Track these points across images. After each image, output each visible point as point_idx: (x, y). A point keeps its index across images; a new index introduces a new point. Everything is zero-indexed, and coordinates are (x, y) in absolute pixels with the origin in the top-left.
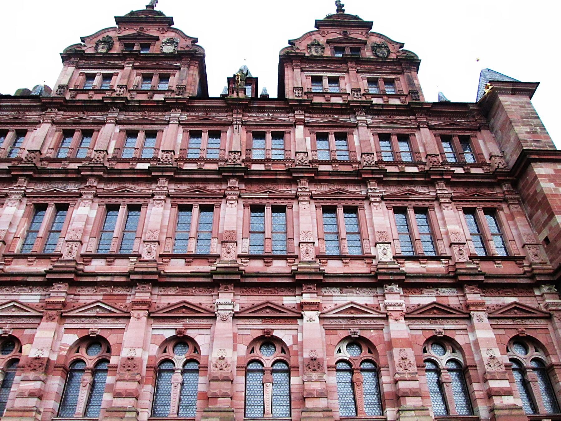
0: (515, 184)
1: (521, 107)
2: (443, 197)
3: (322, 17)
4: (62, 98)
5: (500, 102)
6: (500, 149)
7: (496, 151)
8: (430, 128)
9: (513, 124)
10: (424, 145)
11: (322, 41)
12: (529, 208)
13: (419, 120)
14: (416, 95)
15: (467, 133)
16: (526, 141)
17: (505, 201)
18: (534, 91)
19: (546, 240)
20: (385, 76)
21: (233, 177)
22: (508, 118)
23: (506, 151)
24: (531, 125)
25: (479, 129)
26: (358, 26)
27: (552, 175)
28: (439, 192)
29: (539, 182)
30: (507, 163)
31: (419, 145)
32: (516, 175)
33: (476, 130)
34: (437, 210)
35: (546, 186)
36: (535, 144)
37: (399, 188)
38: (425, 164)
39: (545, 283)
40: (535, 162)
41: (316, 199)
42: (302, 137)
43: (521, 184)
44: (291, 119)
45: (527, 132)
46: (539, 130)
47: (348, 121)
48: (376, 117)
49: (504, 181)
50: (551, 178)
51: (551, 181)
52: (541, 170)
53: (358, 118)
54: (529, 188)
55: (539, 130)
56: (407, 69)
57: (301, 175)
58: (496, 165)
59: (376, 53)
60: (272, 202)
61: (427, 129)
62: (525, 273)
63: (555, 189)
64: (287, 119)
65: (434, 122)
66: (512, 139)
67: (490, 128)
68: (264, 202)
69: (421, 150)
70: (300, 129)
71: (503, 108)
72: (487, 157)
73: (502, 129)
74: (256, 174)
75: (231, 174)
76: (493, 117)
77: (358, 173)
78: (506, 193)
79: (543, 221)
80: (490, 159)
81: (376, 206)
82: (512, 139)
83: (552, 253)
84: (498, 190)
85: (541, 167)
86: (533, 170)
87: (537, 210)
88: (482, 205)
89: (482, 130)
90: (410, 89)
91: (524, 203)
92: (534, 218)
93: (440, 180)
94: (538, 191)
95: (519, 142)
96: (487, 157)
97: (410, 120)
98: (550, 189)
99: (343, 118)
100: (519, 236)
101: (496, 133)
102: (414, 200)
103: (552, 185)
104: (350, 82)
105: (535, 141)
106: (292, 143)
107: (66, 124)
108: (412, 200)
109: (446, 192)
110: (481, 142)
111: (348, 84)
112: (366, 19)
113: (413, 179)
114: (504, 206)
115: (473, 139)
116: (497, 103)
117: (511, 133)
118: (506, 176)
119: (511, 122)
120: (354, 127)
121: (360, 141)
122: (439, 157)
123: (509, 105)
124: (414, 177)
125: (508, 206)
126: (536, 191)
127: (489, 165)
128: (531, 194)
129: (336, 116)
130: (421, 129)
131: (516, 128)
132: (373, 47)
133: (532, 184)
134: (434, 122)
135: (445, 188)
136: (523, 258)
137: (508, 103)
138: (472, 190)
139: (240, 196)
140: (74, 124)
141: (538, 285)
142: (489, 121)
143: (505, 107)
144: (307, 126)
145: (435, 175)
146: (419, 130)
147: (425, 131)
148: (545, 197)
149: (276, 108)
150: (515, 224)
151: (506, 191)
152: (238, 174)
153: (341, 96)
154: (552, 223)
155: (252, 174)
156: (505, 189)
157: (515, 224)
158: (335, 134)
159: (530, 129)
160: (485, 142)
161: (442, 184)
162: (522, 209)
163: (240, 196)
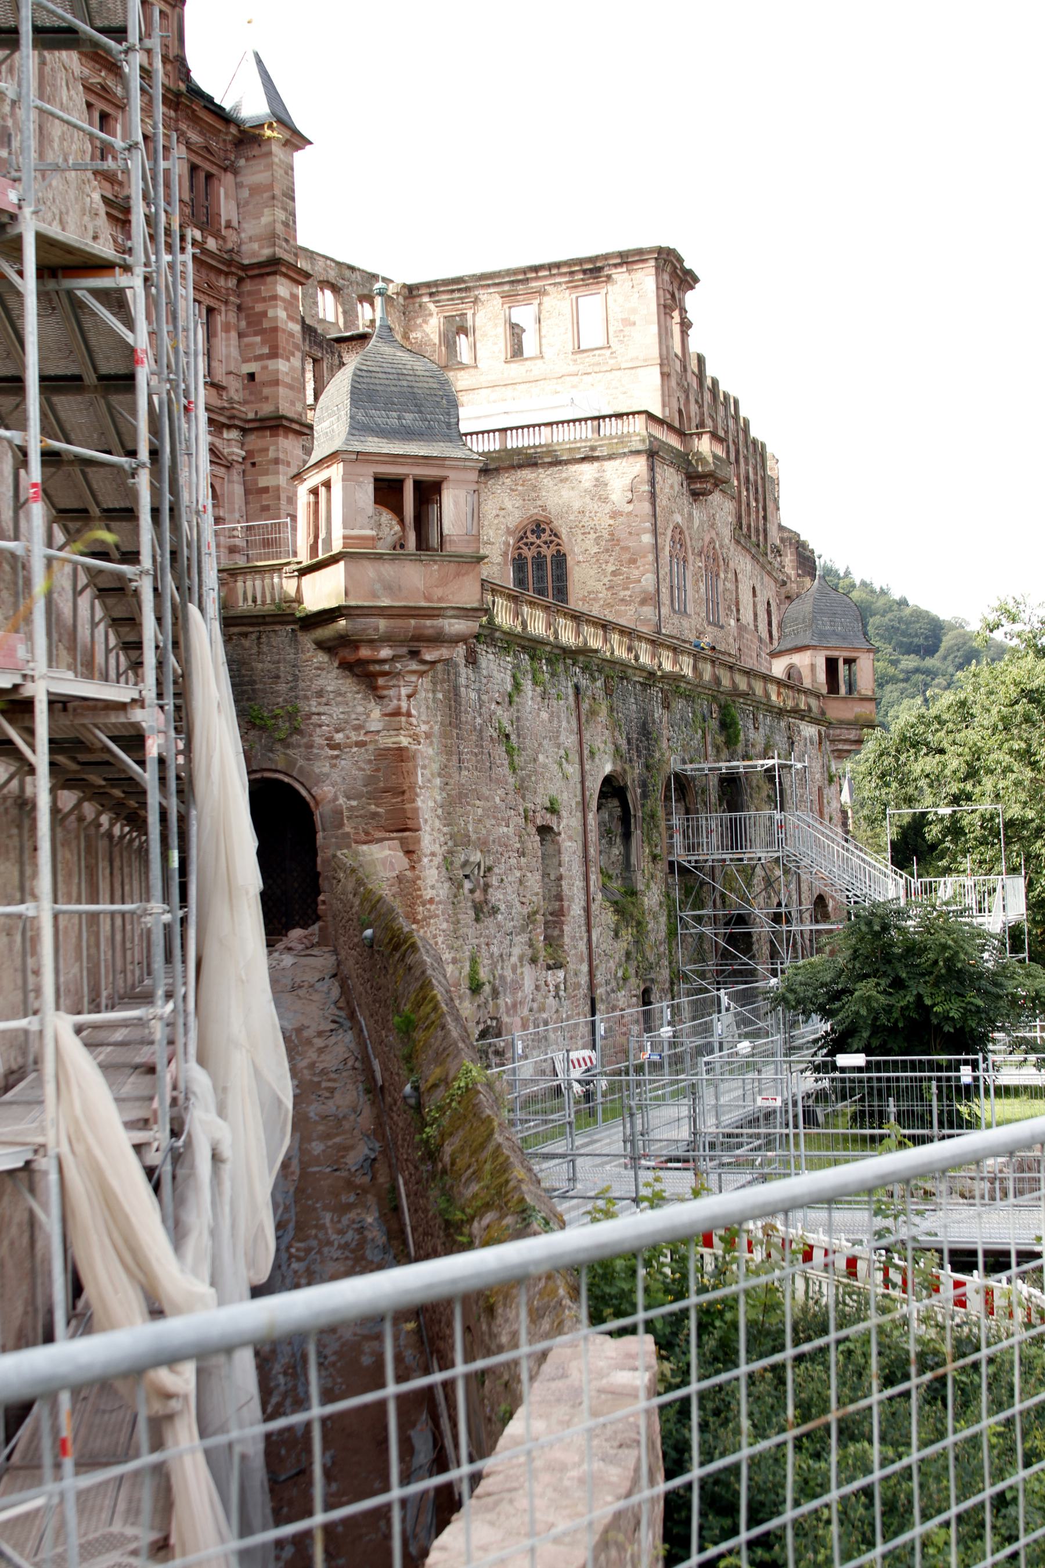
0: (240, 280)
5: (270, 153)
15: (214, 170)
17: (226, 303)
19: (252, 376)
22: (271, 187)
23: (245, 225)
25: (225, 170)
32: (250, 273)
39: (236, 427)
43: (248, 286)
51: (286, 309)
54: (257, 301)
62: (223, 408)
66: (264, 220)
67: (236, 172)
71: (270, 166)
72: (223, 223)
79: (258, 352)
82: (264, 220)
83: (251, 393)
84: (222, 282)
86: (276, 283)
92: (246, 340)
94: (271, 313)
96: (223, 223)
100: (228, 356)
101: (239, 186)
110: (222, 190)
114: (223, 308)
115: (216, 182)
117: (266, 211)
128: (257, 310)
133: (264, 300)
136: (224, 388)
141: (229, 427)
150: (228, 339)
154: (271, 364)
157: (228, 339)
160: (226, 193)
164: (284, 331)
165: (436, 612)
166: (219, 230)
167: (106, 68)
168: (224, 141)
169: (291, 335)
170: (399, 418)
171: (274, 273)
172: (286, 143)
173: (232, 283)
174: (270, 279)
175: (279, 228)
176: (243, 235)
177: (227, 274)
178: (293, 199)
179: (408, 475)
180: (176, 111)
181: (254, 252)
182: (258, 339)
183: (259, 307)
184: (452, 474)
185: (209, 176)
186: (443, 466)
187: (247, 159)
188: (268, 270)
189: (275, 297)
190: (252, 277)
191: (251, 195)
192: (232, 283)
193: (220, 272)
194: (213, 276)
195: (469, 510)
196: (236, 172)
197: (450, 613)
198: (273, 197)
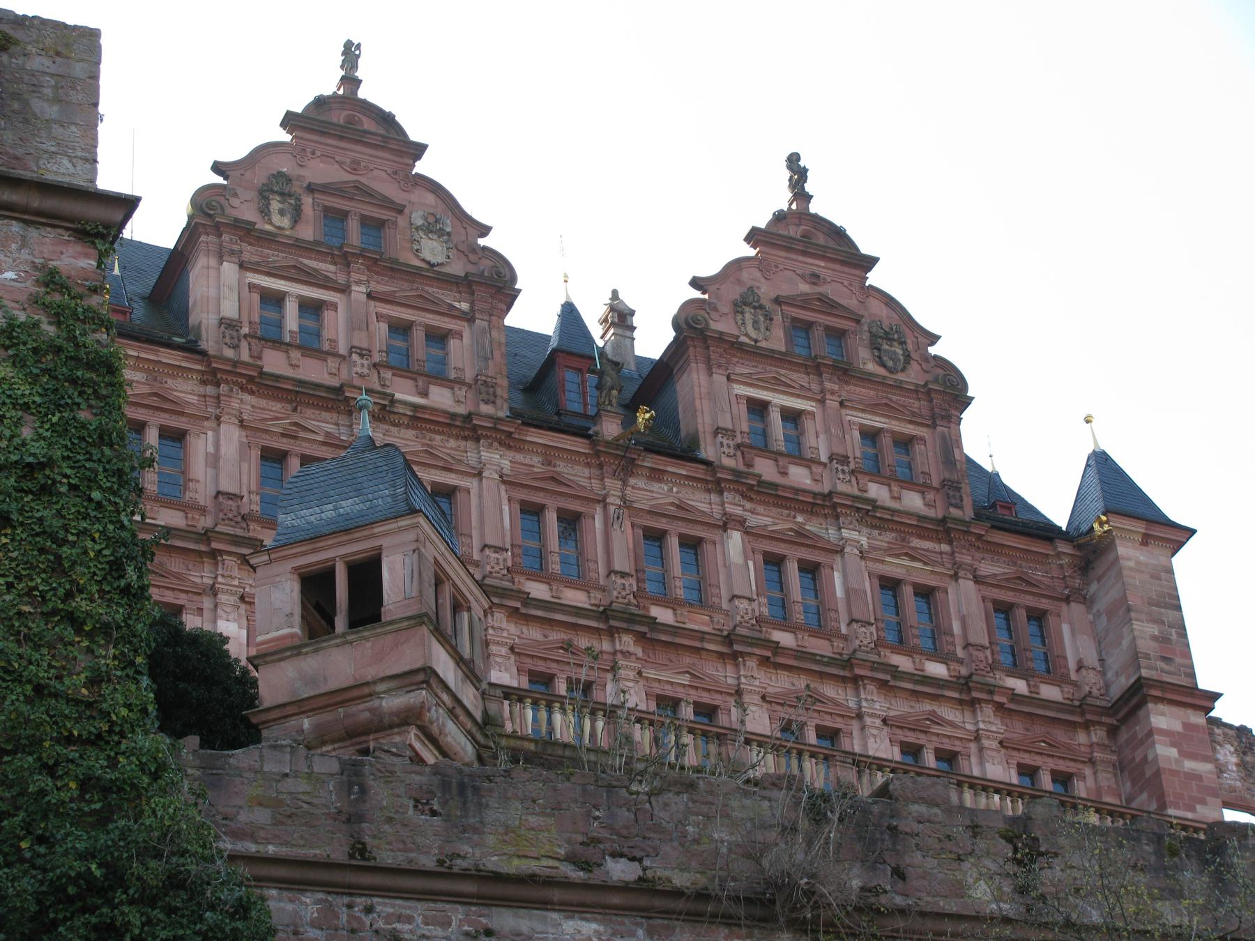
0: (1113, 732)
1: (1152, 577)
2: (988, 738)
3: (762, 221)
4: (257, 366)
5: (1117, 558)
6: (1100, 653)
7: (1091, 659)
8: (978, 580)
9: (1133, 615)
10: (963, 620)
11: (766, 292)
12: (1128, 784)
13: (958, 557)
14: (958, 495)
15: (1044, 604)
16: (1147, 656)
17: (1092, 762)
18: (1181, 544)
20: (896, 426)
21: (627, 631)
22: (1124, 598)
23: (1109, 661)
24: (1163, 622)
25: (1067, 600)
26: (843, 263)
27: (1179, 733)
28: (981, 726)
29: (1154, 743)
30: (1107, 686)
31: (953, 616)
32: (1119, 717)
33: (1060, 600)
34: (974, 760)
35: (1165, 752)
36: (1163, 665)
37: (913, 704)
38: (961, 662)
40: (1156, 703)
41: (771, 702)
42: (740, 561)
43: (1124, 735)
44: (717, 512)
45: (1154, 638)
46: (1174, 637)
47: (823, 533)
48: (876, 532)
49: (1094, 723)
50: (1174, 739)
51: (1173, 745)
52: (1162, 718)
53: (846, 533)
55: (1174, 637)
56: (943, 418)
57: (749, 650)
58: (1087, 688)
59: (880, 358)
60: (694, 696)
61: (971, 583)
63: (1176, 761)
64: (704, 507)
65: (988, 568)
66: (1125, 643)
67: (1088, 602)
68: (680, 693)
69: (956, 628)
70: (735, 539)
71: (1120, 575)
72: (1072, 665)
73: (1110, 613)
74: (665, 632)
75: (624, 625)
76: (1099, 580)
77: (848, 663)
78: (1096, 748)
80: (1078, 671)
81: (874, 736)
82: (1125, 643)
84: (1082, 737)
85: (1163, 714)
86: (1148, 716)
87: (1141, 792)
88: (1052, 764)
89: (1073, 604)
90: (947, 475)
91: (1122, 771)
93: (987, 701)
94: (1150, 757)
95: (1135, 658)
96: (1072, 665)
97: (941, 553)
98: (1169, 759)
99: (813, 526)
101: (1098, 615)
102: (938, 735)
103: (1173, 752)
104: (827, 431)
105: (1164, 659)
106: (722, 570)
107: (266, 431)
108: (933, 734)
109: (994, 729)
110: (1066, 628)
111: (822, 437)
112: (865, 249)
113: (940, 692)
114: (1088, 771)
116: (1111, 557)
118: (1101, 714)
119: (1129, 610)
120: (837, 552)
121: (848, 591)
122: (988, 653)
123: (1131, 569)
124: (941, 687)
125: (1095, 773)
126: (1146, 757)
127: (1075, 684)
128: (1137, 760)
129: (800, 519)
130: (961, 581)
131: (1136, 625)
132: (873, 336)
133: (1142, 742)
134: (988, 568)
135: (992, 719)
137: (1131, 564)
138: (1039, 730)
139: (640, 673)
140: (283, 435)
142: (1088, 584)
143: (1125, 573)
144: (747, 532)
145: (981, 690)
146: (956, 581)
147: (967, 586)
148: (1158, 773)
149: (687, 477)
151: (1098, 744)
152: (638, 628)
153: (809, 467)
155: (659, 631)
156: (1094, 739)
158: (800, 561)
159: (1161, 632)
160: (1073, 631)
161: (988, 710)
162: (1117, 783)
163: (640, 673)
164: (1174, 773)
165: (366, 690)
166: (1068, 675)
167: (803, 511)
168: (1061, 566)
169: (1196, 777)
170: (335, 509)
171: (1141, 704)
172: (1146, 540)
173: (1098, 735)
174: (1141, 713)
175: (1145, 645)
176: (1110, 675)
177: (1086, 726)
178: (1178, 608)
179: (333, 559)
180: (950, 543)
181: (1121, 684)
182: (1145, 795)
183: (1138, 756)
184: (385, 542)
185: (1037, 617)
186: (373, 536)
187: (1099, 580)
188: (1135, 701)
189: (1150, 733)
190: (1124, 720)
191: (1109, 620)
192: (1098, 735)
193: (1072, 725)
194: (1060, 735)
195: (408, 572)
196: (1088, 602)
197: (381, 687)
198: (1129, 610)
